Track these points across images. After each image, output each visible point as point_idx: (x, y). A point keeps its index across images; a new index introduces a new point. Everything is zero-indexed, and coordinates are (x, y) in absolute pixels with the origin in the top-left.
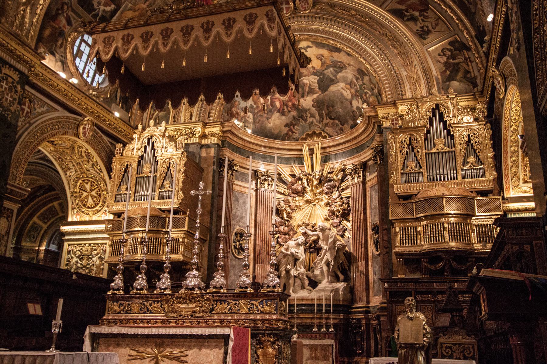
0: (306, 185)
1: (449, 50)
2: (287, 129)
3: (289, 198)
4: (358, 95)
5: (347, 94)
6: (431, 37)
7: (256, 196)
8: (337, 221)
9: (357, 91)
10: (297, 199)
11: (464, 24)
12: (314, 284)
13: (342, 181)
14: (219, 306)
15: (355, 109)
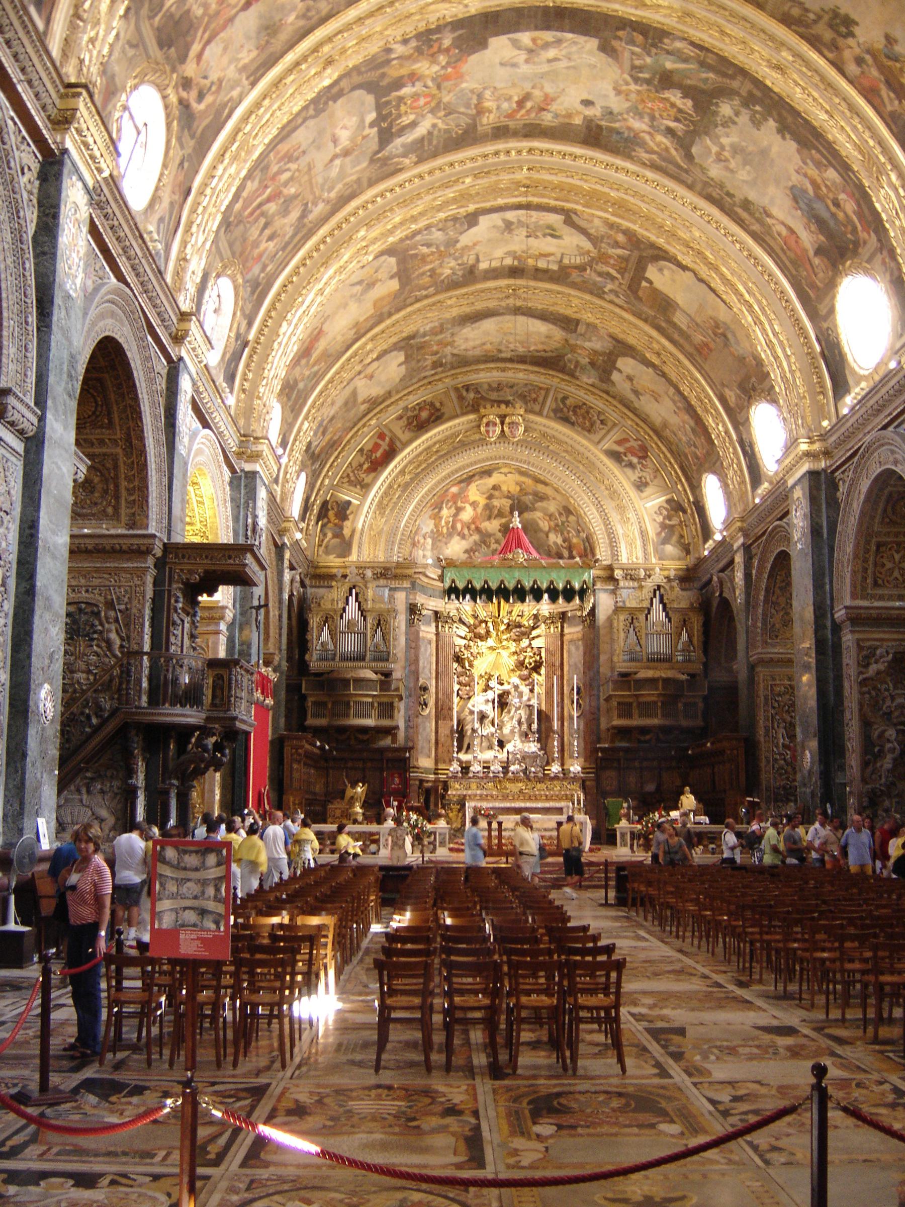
0: (491, 629)
1: (666, 509)
2: (466, 555)
3: (472, 643)
4: (560, 529)
5: (544, 525)
6: (649, 490)
7: (437, 641)
8: (526, 672)
9: (557, 525)
10: (480, 643)
11: (683, 485)
12: (501, 744)
13: (534, 628)
14: (539, 786)
15: (551, 542)
